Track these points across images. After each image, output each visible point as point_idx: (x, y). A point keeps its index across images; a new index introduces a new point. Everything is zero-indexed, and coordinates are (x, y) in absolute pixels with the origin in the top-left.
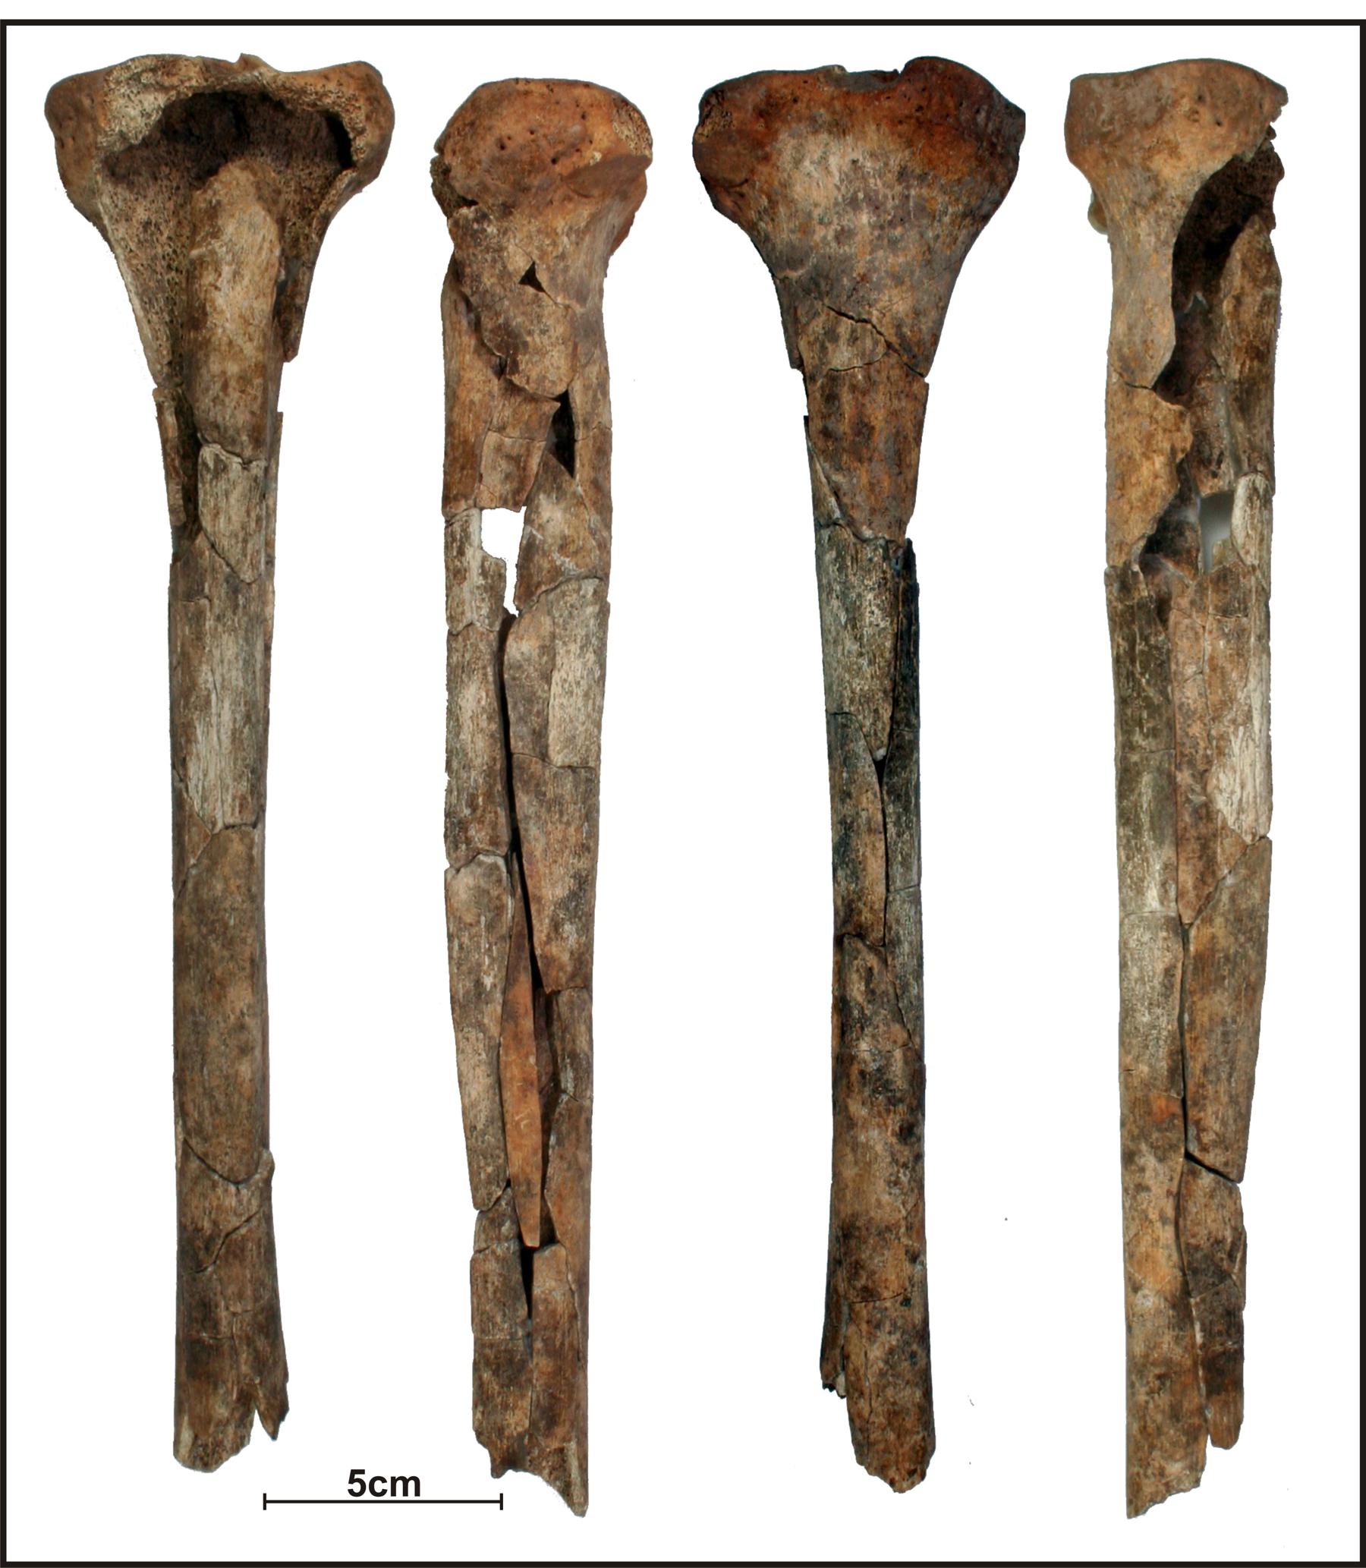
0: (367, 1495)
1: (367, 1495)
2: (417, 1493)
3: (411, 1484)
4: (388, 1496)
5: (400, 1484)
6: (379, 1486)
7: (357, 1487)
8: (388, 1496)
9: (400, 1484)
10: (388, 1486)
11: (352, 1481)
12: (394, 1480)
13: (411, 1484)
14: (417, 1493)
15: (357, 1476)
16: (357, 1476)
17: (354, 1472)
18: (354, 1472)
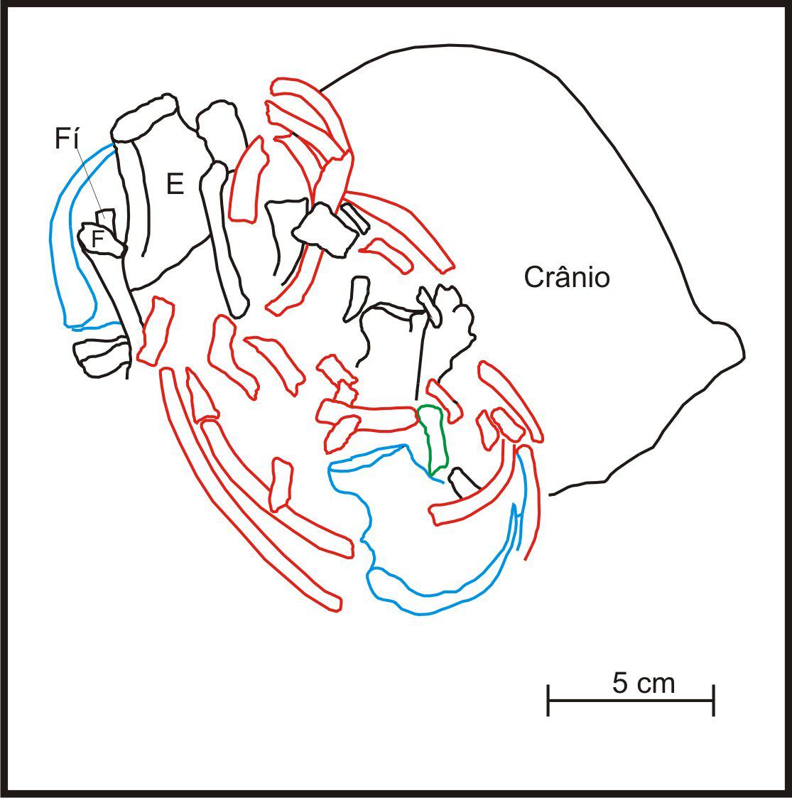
3: (668, 683)
5: (659, 683)
6: (645, 685)
9: (659, 683)
10: (651, 685)
12: (655, 680)
13: (668, 683)
14: (673, 691)
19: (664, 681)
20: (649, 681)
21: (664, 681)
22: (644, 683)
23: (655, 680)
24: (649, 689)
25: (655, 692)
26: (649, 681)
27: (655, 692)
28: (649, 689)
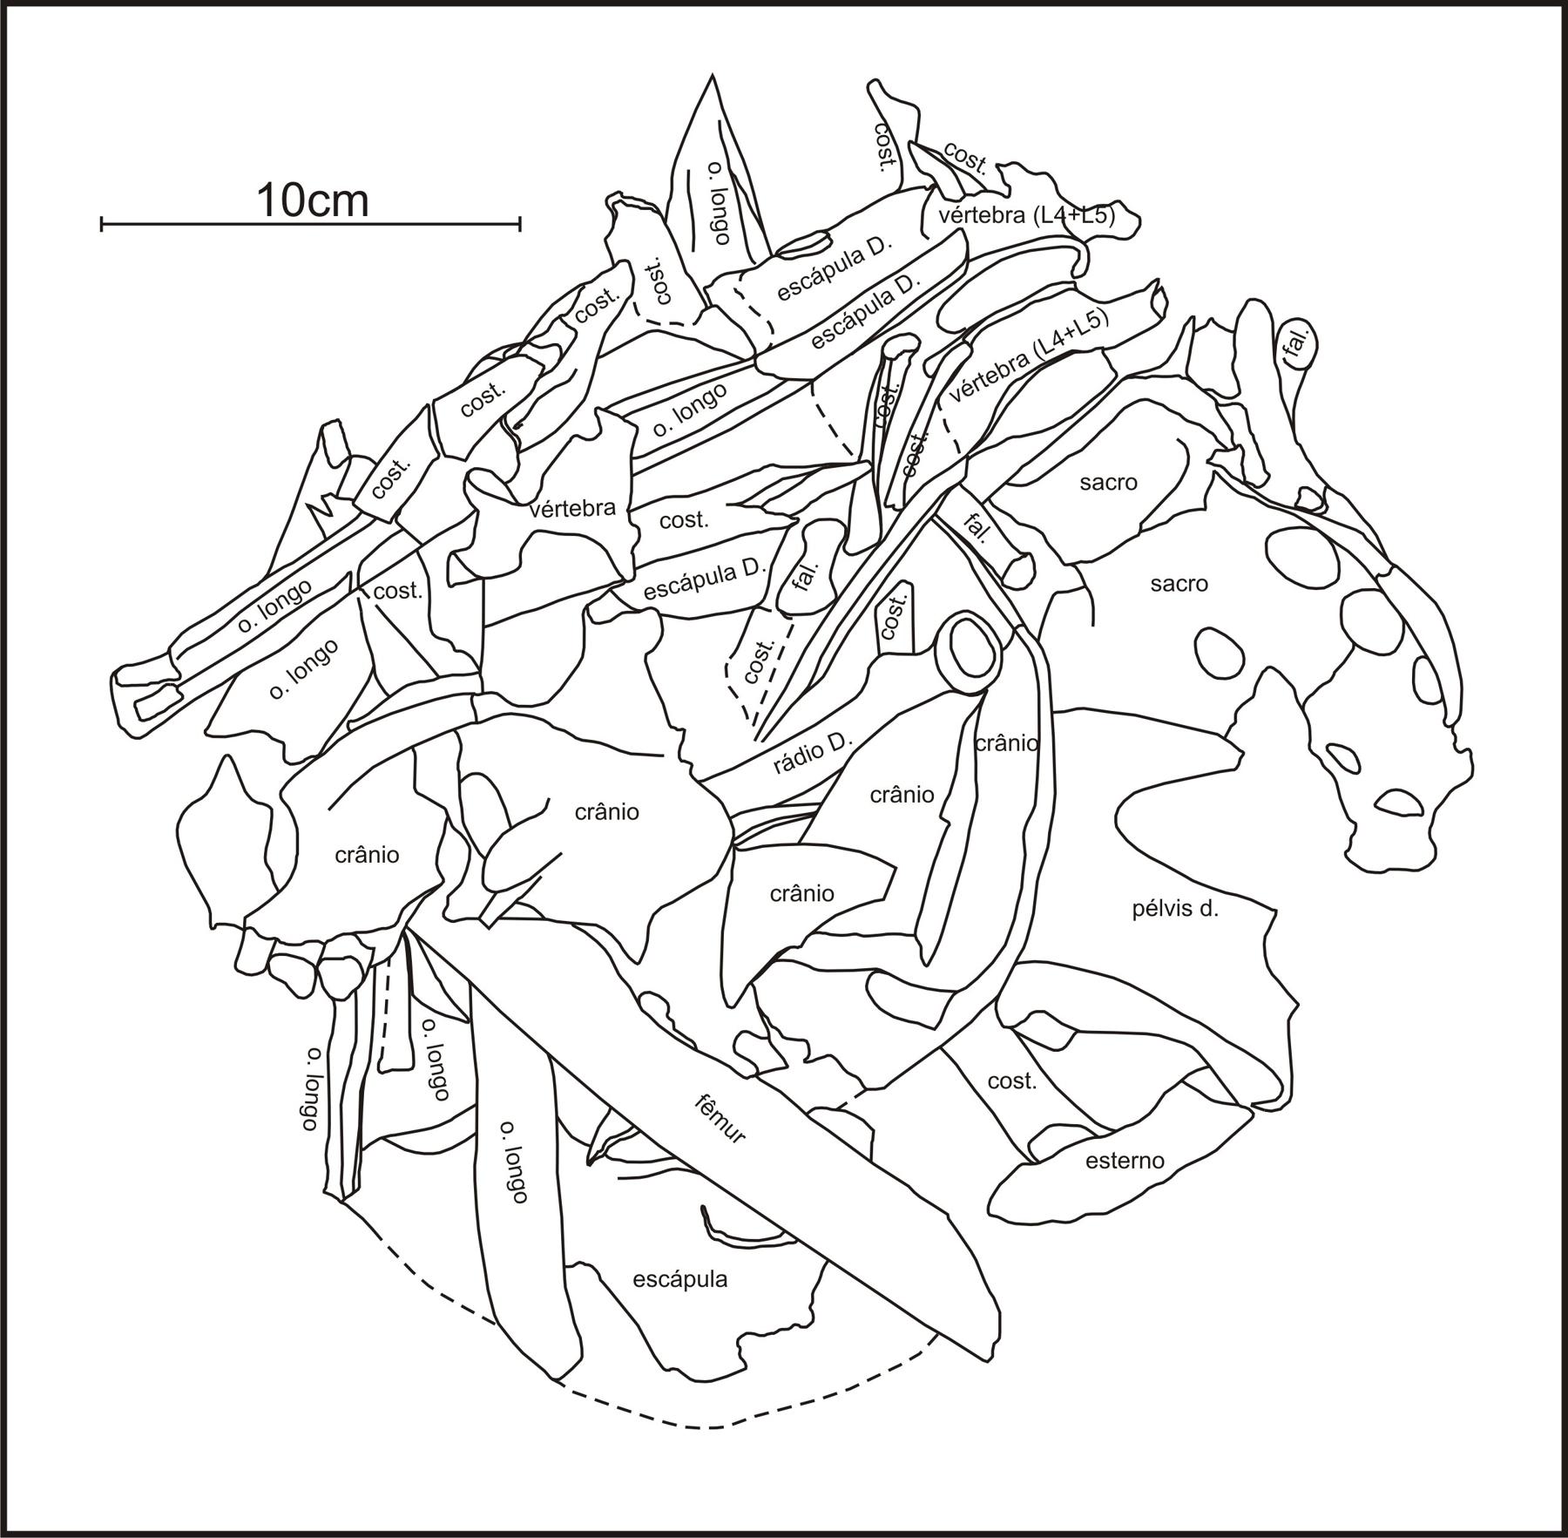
0: (306, 216)
1: (306, 216)
2: (365, 214)
3: (358, 200)
4: (330, 218)
5: (344, 200)
6: (320, 204)
8: (330, 218)
9: (344, 200)
10: (330, 203)
12: (337, 196)
13: (358, 200)
14: (365, 214)
19: (351, 197)
20: (327, 197)
21: (351, 197)
22: (319, 198)
23: (337, 196)
24: (328, 210)
25: (336, 214)
26: (327, 197)
27: (336, 214)
28: (328, 210)
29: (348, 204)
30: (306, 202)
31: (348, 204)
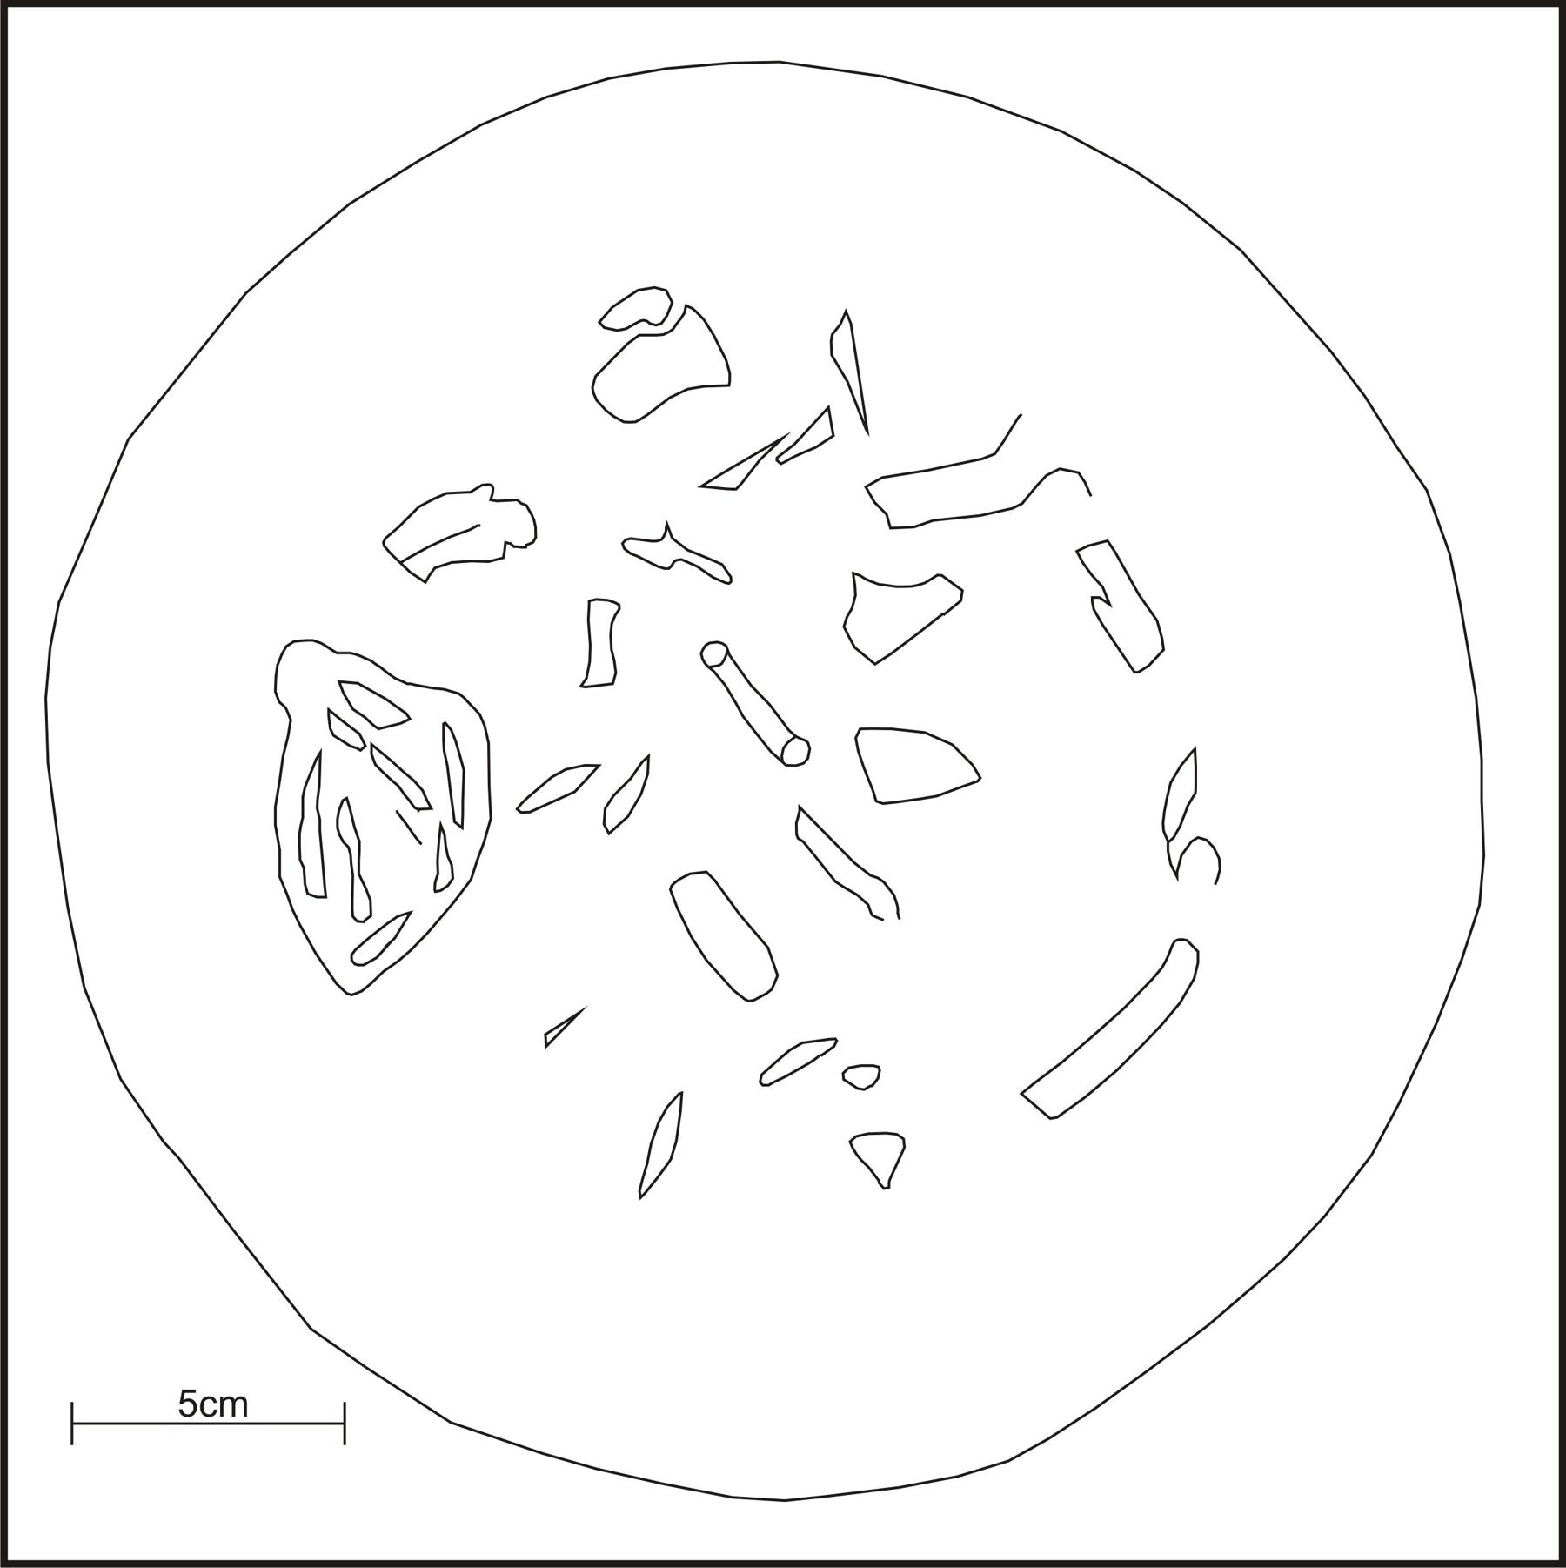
0: (198, 1417)
1: (198, 1417)
3: (240, 1404)
4: (217, 1418)
5: (228, 1404)
6: (209, 1407)
7: (188, 1408)
8: (217, 1418)
9: (228, 1404)
10: (217, 1406)
11: (182, 1401)
12: (222, 1400)
13: (240, 1404)
15: (187, 1396)
16: (187, 1396)
17: (184, 1392)
18: (184, 1392)
19: (234, 1401)
21: (234, 1401)
22: (208, 1403)
23: (222, 1400)
29: (228, 1409)
30: (198, 1407)
31: (228, 1409)
